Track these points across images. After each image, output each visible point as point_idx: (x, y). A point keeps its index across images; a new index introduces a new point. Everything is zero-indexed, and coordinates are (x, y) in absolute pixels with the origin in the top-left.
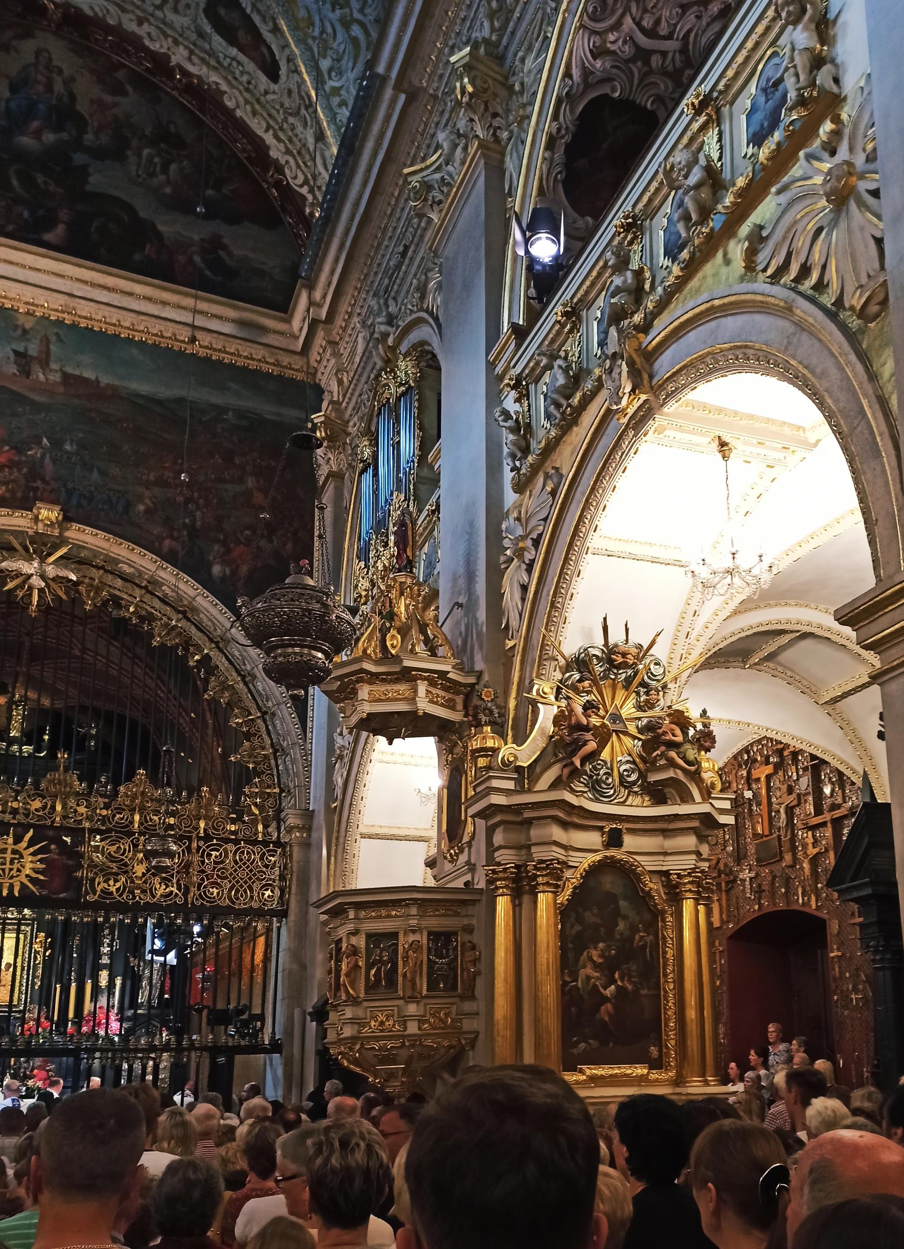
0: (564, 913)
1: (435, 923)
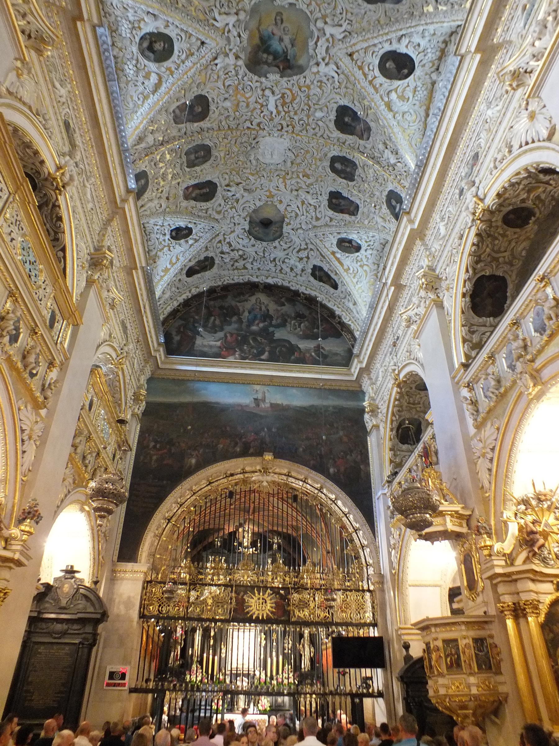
0: (543, 627)
1: (472, 633)
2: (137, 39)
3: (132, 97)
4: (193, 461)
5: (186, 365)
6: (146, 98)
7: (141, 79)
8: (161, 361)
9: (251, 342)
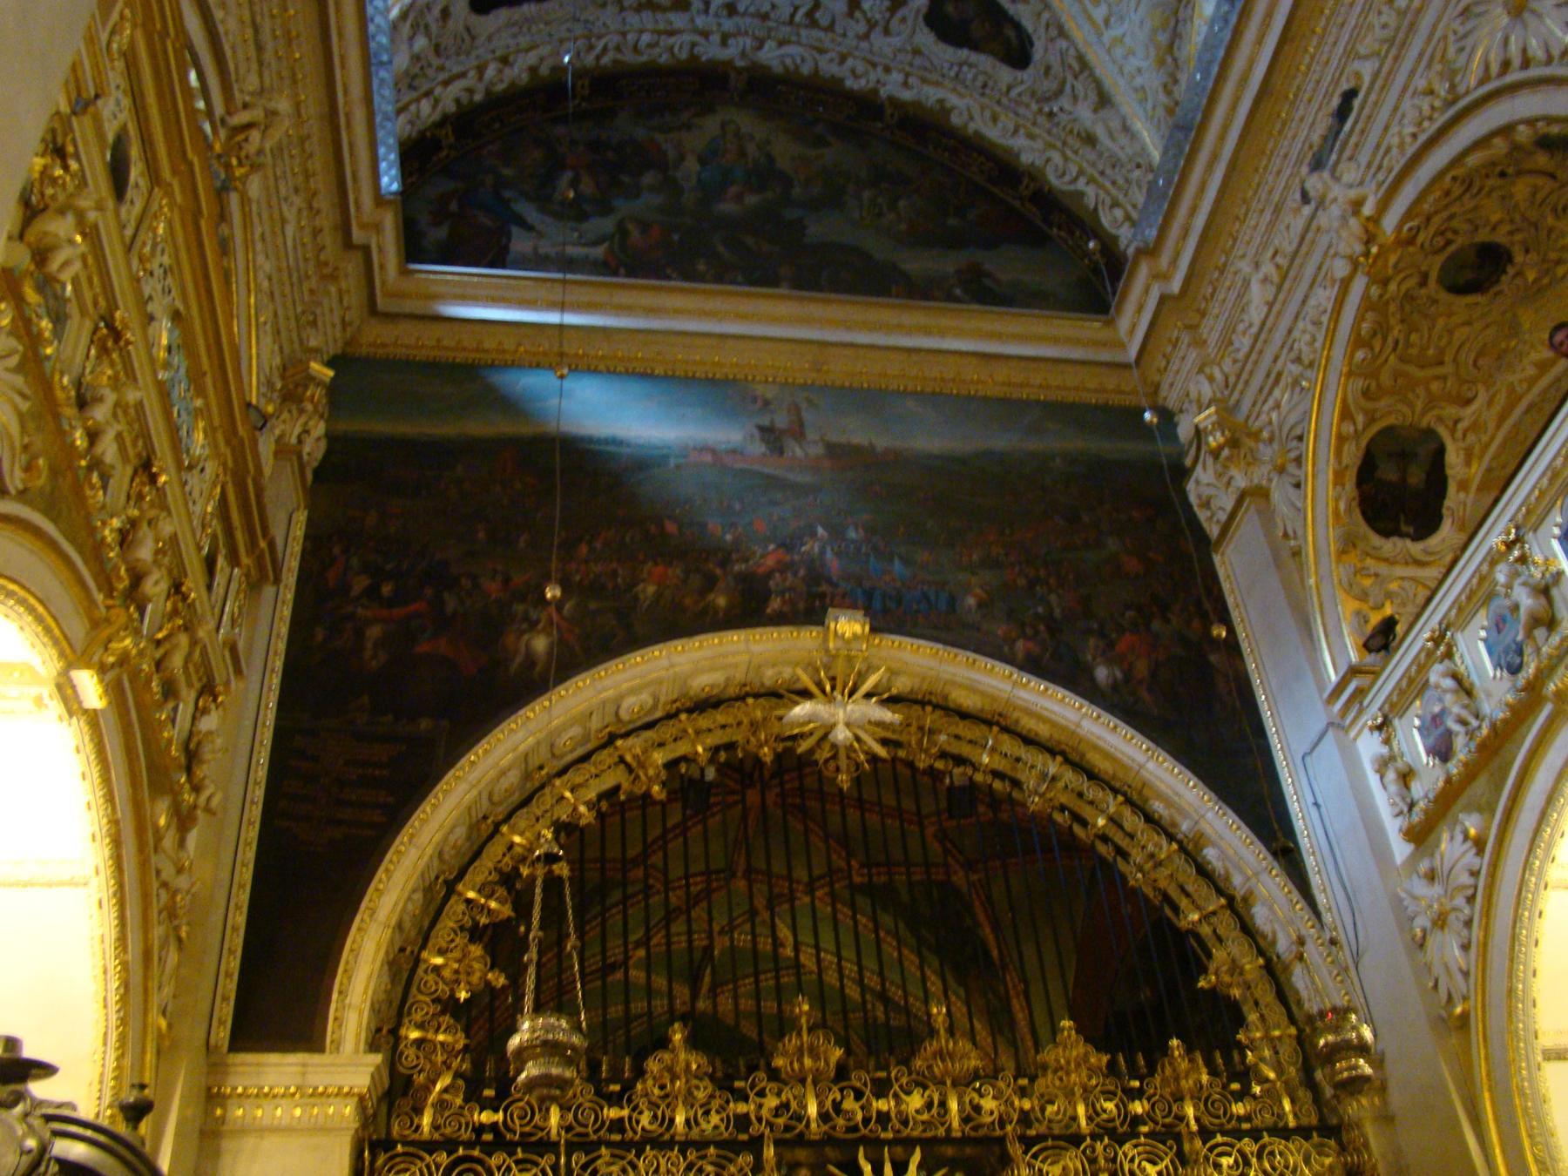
4: (540, 644)
5: (483, 304)
8: (383, 283)
9: (721, 249)
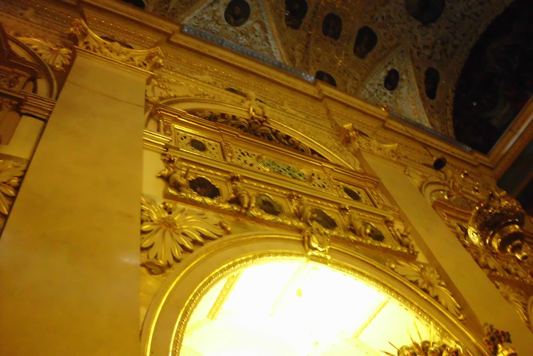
2: (226, 23)
3: (262, 50)
6: (267, 39)
7: (252, 36)
